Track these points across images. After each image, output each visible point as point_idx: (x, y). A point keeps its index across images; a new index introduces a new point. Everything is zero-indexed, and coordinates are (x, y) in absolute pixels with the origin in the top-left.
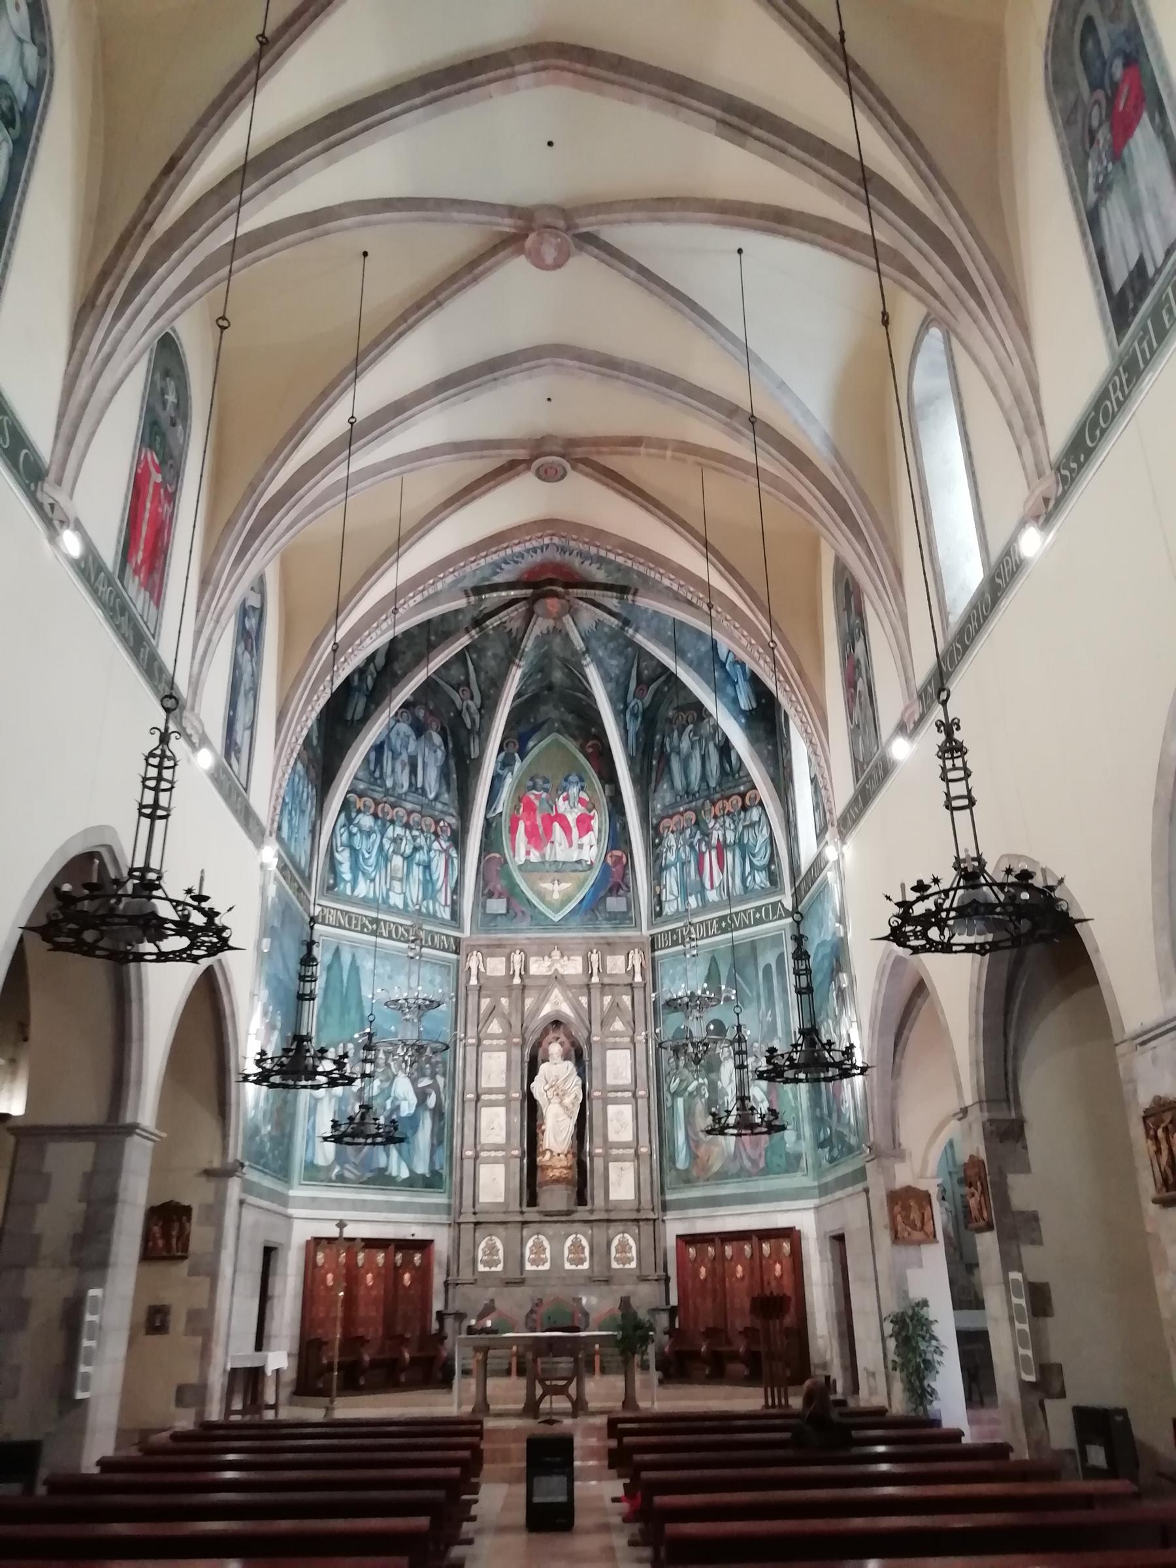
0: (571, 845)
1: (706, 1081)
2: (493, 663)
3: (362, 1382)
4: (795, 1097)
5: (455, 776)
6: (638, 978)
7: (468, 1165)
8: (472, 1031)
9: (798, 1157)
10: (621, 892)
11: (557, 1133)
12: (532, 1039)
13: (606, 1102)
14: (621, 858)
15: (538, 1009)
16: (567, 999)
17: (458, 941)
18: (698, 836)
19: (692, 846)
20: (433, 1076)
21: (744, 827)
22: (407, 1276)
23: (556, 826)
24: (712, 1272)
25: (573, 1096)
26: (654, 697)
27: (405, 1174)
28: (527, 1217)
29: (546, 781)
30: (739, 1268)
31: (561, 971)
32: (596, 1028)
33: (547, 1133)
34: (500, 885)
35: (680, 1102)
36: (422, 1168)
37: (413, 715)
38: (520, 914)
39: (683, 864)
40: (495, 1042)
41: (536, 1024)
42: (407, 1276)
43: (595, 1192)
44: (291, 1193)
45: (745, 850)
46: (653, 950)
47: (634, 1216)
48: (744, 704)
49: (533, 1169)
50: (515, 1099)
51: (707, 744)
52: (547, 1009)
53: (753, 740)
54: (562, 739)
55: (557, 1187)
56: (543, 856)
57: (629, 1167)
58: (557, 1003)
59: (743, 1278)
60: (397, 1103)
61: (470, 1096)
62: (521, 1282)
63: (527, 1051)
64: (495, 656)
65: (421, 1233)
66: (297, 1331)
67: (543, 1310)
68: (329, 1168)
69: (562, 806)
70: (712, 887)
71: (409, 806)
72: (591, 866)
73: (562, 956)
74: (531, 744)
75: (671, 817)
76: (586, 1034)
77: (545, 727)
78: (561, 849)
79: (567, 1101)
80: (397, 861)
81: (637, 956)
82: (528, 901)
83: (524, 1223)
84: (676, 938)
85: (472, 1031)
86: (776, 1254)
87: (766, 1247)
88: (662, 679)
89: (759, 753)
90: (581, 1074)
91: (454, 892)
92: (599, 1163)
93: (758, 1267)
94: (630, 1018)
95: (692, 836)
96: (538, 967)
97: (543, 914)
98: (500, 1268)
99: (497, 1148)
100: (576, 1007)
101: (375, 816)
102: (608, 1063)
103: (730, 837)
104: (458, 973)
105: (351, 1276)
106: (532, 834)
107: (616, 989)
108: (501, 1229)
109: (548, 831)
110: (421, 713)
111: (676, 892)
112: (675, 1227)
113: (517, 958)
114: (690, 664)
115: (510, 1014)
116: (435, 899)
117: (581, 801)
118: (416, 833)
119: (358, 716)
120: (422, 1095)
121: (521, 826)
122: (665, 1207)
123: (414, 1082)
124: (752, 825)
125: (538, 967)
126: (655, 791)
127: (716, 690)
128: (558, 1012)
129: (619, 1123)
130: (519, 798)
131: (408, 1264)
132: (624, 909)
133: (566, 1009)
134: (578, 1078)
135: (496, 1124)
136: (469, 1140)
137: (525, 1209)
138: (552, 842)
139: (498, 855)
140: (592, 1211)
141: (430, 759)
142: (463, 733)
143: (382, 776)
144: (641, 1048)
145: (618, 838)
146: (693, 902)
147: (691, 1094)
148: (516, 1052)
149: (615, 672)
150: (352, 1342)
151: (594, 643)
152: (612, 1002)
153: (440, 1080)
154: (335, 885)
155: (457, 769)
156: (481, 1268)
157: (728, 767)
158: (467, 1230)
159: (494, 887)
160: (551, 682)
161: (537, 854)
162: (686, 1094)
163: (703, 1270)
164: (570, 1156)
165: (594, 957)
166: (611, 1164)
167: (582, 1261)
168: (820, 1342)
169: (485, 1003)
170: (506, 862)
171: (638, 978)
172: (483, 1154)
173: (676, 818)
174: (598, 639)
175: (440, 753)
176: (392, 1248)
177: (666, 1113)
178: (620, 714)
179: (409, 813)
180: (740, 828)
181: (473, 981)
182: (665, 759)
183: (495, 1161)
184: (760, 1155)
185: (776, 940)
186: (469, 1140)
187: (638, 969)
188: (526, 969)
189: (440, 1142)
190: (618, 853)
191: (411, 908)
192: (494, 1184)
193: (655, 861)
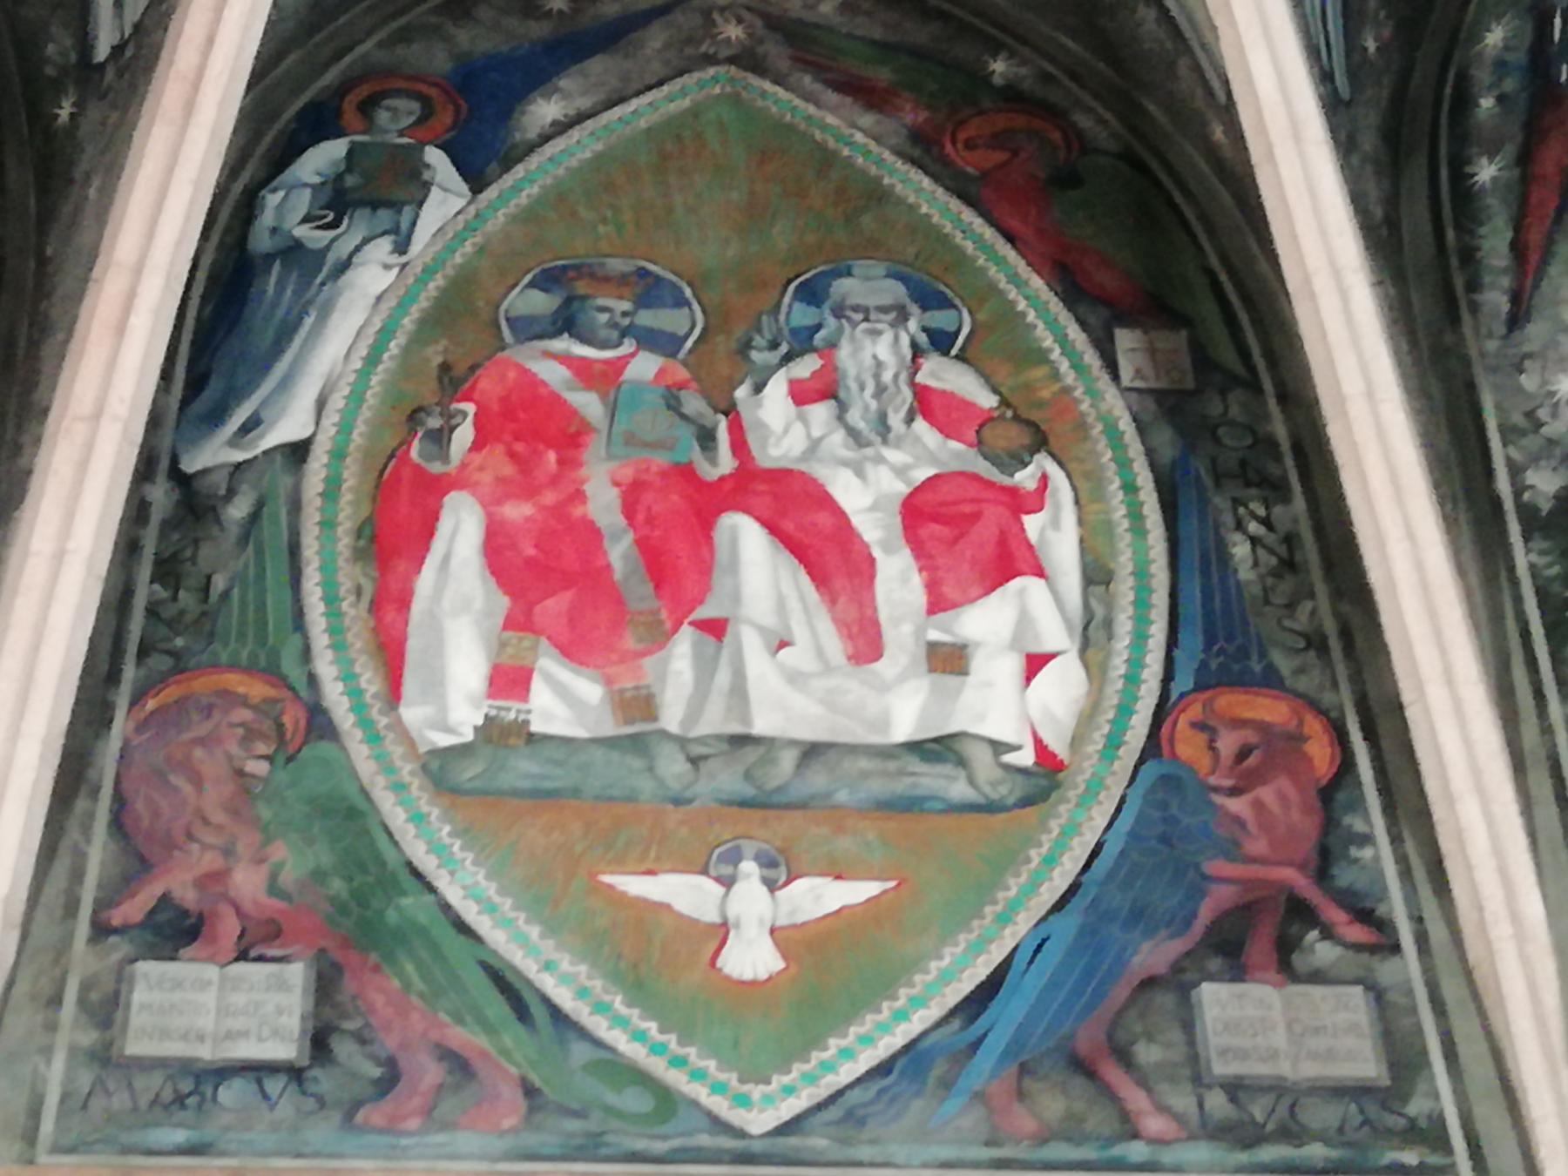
0: (865, 642)
10: (1323, 952)
14: (1297, 738)
23: (745, 540)
29: (649, 290)
38: (432, 1073)
54: (775, 98)
56: (639, 705)
69: (780, 424)
74: (545, 110)
77: (655, 38)
78: (774, 661)
106: (547, 581)
109: (679, 567)
117: (926, 403)
121: (461, 527)
126: (1517, 319)
132: (1367, 1065)
138: (715, 628)
139: (258, 690)
159: (215, 879)
161: (589, 689)
170: (319, 724)
190: (1271, 710)
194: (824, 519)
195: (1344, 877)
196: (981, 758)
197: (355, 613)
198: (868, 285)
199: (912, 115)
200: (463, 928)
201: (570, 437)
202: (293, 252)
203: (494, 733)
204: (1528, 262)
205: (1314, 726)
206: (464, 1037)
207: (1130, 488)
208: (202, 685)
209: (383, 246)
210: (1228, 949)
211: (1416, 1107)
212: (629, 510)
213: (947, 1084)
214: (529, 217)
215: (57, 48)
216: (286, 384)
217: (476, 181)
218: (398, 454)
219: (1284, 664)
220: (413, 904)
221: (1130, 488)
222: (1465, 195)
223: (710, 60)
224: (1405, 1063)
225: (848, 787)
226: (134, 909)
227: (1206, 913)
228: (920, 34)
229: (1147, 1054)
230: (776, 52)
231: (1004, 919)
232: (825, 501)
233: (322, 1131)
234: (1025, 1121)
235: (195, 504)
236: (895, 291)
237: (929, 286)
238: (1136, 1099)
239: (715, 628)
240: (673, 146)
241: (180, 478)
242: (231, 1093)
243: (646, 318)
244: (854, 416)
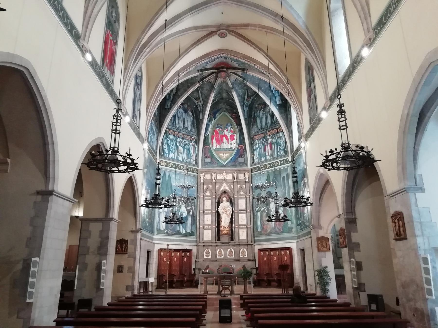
2: (206, 92)
3: (174, 286)
4: (291, 212)
7: (201, 230)
8: (202, 194)
9: (292, 228)
11: (225, 221)
12: (218, 197)
13: (239, 213)
15: (220, 188)
16: (228, 186)
17: (197, 170)
18: (264, 141)
19: (263, 143)
20: (191, 206)
22: (185, 259)
23: (224, 138)
24: (268, 259)
27: (184, 232)
28: (217, 244)
29: (221, 125)
30: (275, 258)
32: (236, 194)
34: (209, 155)
35: (259, 213)
36: (189, 231)
37: (184, 107)
39: (260, 148)
41: (219, 193)
42: (185, 259)
44: (154, 237)
45: (278, 144)
46: (252, 172)
47: (246, 244)
48: (278, 103)
49: (219, 231)
52: (222, 188)
53: (281, 113)
54: (226, 113)
56: (221, 147)
57: (245, 231)
58: (225, 187)
59: (276, 260)
61: (202, 212)
62: (216, 261)
63: (217, 200)
64: (207, 89)
65: (189, 248)
66: (157, 273)
67: (222, 268)
68: (164, 230)
69: (226, 132)
71: (183, 133)
72: (234, 149)
74: (217, 115)
75: (257, 135)
78: (226, 145)
79: (228, 213)
80: (180, 148)
81: (247, 174)
83: (217, 245)
84: (258, 169)
85: (202, 194)
86: (285, 254)
87: (282, 252)
88: (254, 96)
89: (282, 117)
91: (196, 156)
92: (237, 229)
93: (280, 258)
94: (245, 191)
95: (263, 141)
98: (210, 257)
99: (209, 225)
100: (230, 188)
101: (174, 135)
103: (274, 141)
104: (197, 179)
105: (171, 258)
106: (217, 141)
107: (242, 183)
108: (210, 247)
109: (222, 140)
110: (186, 106)
112: (257, 247)
113: (214, 175)
114: (263, 91)
116: (191, 159)
117: (231, 131)
118: (185, 140)
119: (169, 107)
120: (188, 211)
121: (214, 138)
122: (255, 242)
123: (186, 208)
124: (280, 137)
125: (220, 177)
127: (271, 99)
128: (225, 189)
129: (242, 219)
130: (214, 131)
131: (185, 255)
133: (227, 188)
135: (209, 219)
136: (201, 223)
137: (217, 241)
140: (235, 242)
142: (198, 112)
143: (175, 124)
144: (248, 199)
145: (242, 141)
146: (263, 159)
148: (214, 200)
149: (241, 94)
150: (171, 276)
151: (235, 86)
152: (240, 186)
153: (193, 207)
154: (164, 154)
156: (205, 257)
158: (201, 247)
163: (265, 258)
165: (235, 174)
167: (232, 255)
168: (297, 277)
169: (205, 187)
171: (247, 180)
172: (205, 227)
174: (236, 84)
175: (191, 118)
176: (181, 251)
177: (255, 217)
178: (242, 106)
179: (183, 135)
181: (202, 181)
183: (208, 229)
185: (286, 170)
186: (201, 223)
187: (247, 178)
188: (216, 178)
189: (194, 224)
190: (242, 146)
191: (185, 161)
192: (208, 235)
203: (216, 148)
204: (253, 125)
222: (251, 120)
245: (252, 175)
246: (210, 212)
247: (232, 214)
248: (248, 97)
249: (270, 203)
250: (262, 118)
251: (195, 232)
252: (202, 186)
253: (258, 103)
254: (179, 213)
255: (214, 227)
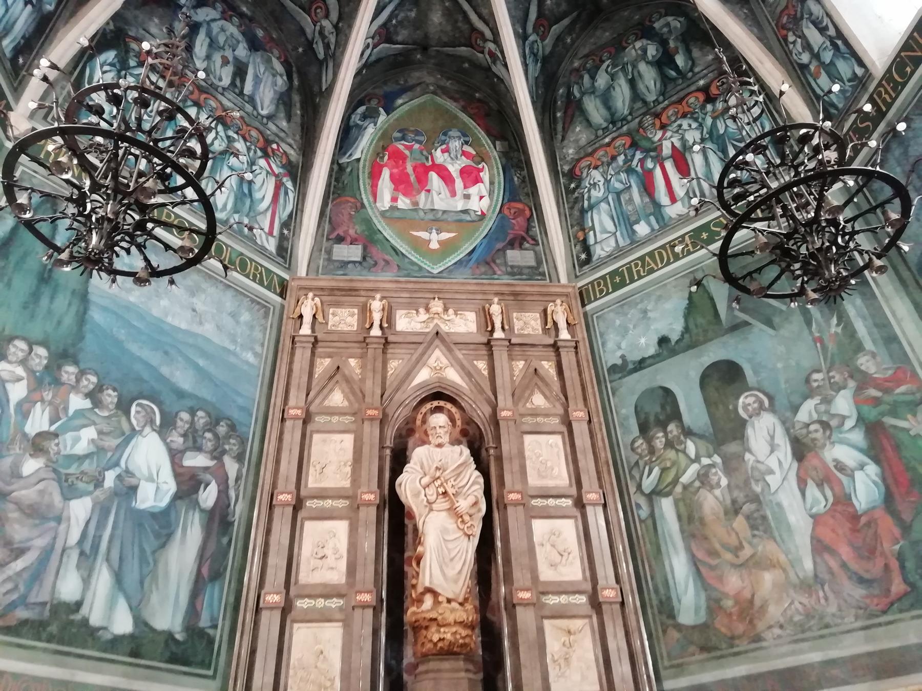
0: (453, 194)
1: (717, 459)
5: (299, 112)
6: (564, 335)
7: (270, 622)
10: (527, 245)
11: (444, 559)
12: (399, 416)
14: (524, 210)
15: (409, 374)
18: (639, 155)
19: (630, 171)
20: (218, 454)
21: (715, 119)
23: (434, 176)
25: (471, 499)
26: (555, 45)
27: (123, 624)
29: (417, 133)
31: (445, 328)
32: (504, 400)
33: (426, 562)
35: (667, 506)
36: (167, 617)
38: (382, 263)
40: (335, 419)
43: (525, 674)
46: (583, 305)
50: (368, 504)
51: (634, 66)
52: (423, 375)
54: (438, 100)
55: (446, 665)
56: (416, 204)
60: (133, 481)
63: (390, 433)
69: (439, 157)
70: (673, 200)
73: (446, 310)
74: (400, 101)
75: (591, 154)
76: (487, 410)
77: (418, 89)
78: (438, 196)
79: (463, 504)
82: (395, 249)
84: (618, 280)
85: (296, 399)
88: (566, 22)
90: (482, 467)
91: (285, 225)
92: (525, 617)
94: (556, 386)
96: (407, 322)
97: (413, 263)
99: (328, 592)
102: (527, 453)
106: (401, 183)
109: (422, 180)
110: (260, 33)
111: (610, 226)
113: (376, 305)
115: (363, 380)
120: (189, 484)
123: (175, 456)
126: (563, 140)
128: (441, 380)
129: (554, 549)
132: (533, 263)
133: (453, 376)
134: (477, 473)
135: (330, 550)
136: (275, 574)
138: (429, 191)
139: (352, 200)
141: (267, 79)
144: (581, 430)
147: (685, 487)
148: (371, 432)
153: (231, 467)
155: (302, 108)
157: (673, 73)
159: (346, 232)
160: (426, 36)
161: (408, 201)
162: (679, 489)
164: (469, 606)
166: (547, 623)
169: (323, 365)
170: (363, 206)
171: (564, 335)
172: (302, 604)
173: (601, 153)
178: (521, 38)
180: (709, 121)
181: (306, 330)
182: (574, 108)
183: (324, 617)
184: (887, 567)
186: (275, 574)
187: (562, 325)
189: (216, 575)
190: (520, 206)
193: (572, 208)
194: (446, 173)
195: (531, 233)
196: (472, 213)
197: (368, 187)
198: (454, 133)
199: (462, 103)
200: (387, 240)
201: (404, 158)
202: (357, 125)
203: (392, 208)
205: (527, 209)
206: (388, 257)
207: (498, 168)
208: (343, 199)
209: (372, 125)
210: (511, 245)
211: (541, 270)
212: (414, 170)
213: (466, 266)
214: (397, 120)
215: (316, 89)
216: (356, 148)
217: (388, 114)
218: (375, 161)
219: (522, 198)
220: (379, 236)
221: (498, 168)
223: (428, 93)
224: (539, 262)
225: (450, 217)
226: (333, 236)
227: (508, 239)
228: (464, 89)
229: (498, 261)
230: (439, 92)
231: (475, 240)
232: (447, 170)
233: (365, 272)
234: (478, 271)
235: (341, 168)
236: (459, 134)
237: (465, 133)
238: (496, 269)
239: (429, 191)
240: (422, 107)
241: (338, 164)
242: (350, 266)
243: (417, 138)
244: (452, 155)
245: (585, 315)
246: (341, 504)
247: (488, 520)
248: (540, 14)
249: (742, 424)
250: (610, 88)
251: (220, 634)
252: (302, 356)
253: (585, 51)
254: (110, 479)
255: (367, 598)
